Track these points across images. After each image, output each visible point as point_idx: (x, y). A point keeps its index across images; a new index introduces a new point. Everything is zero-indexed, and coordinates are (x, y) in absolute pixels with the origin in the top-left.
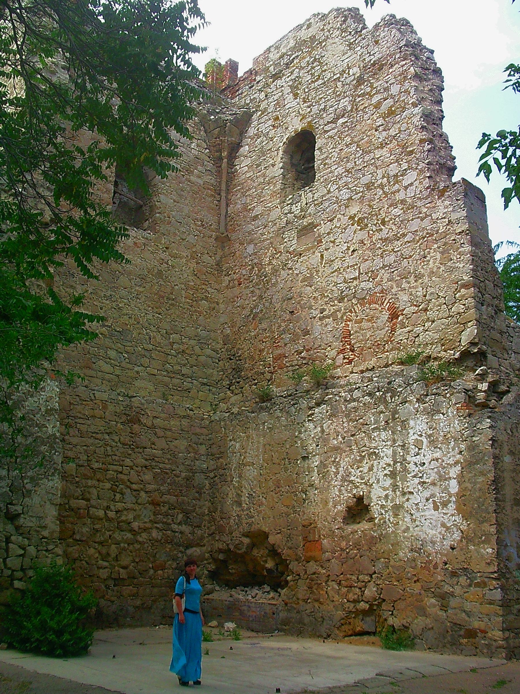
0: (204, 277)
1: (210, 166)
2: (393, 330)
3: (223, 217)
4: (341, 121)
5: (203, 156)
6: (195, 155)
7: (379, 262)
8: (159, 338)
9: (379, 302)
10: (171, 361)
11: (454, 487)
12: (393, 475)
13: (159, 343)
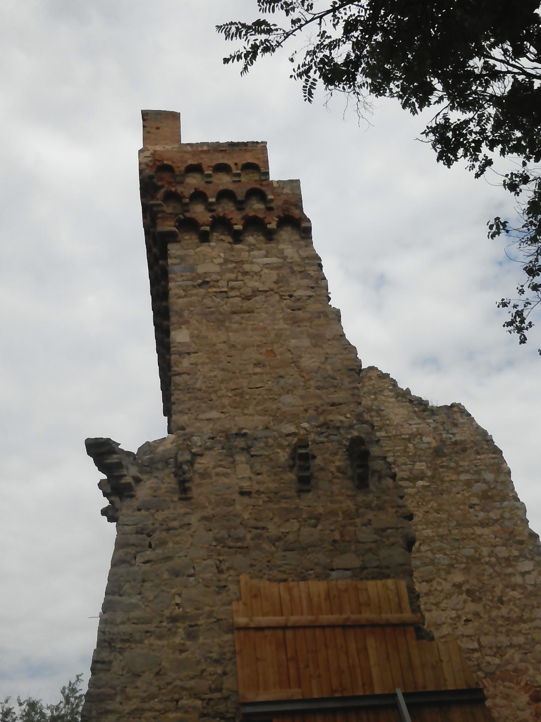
4: (420, 483)
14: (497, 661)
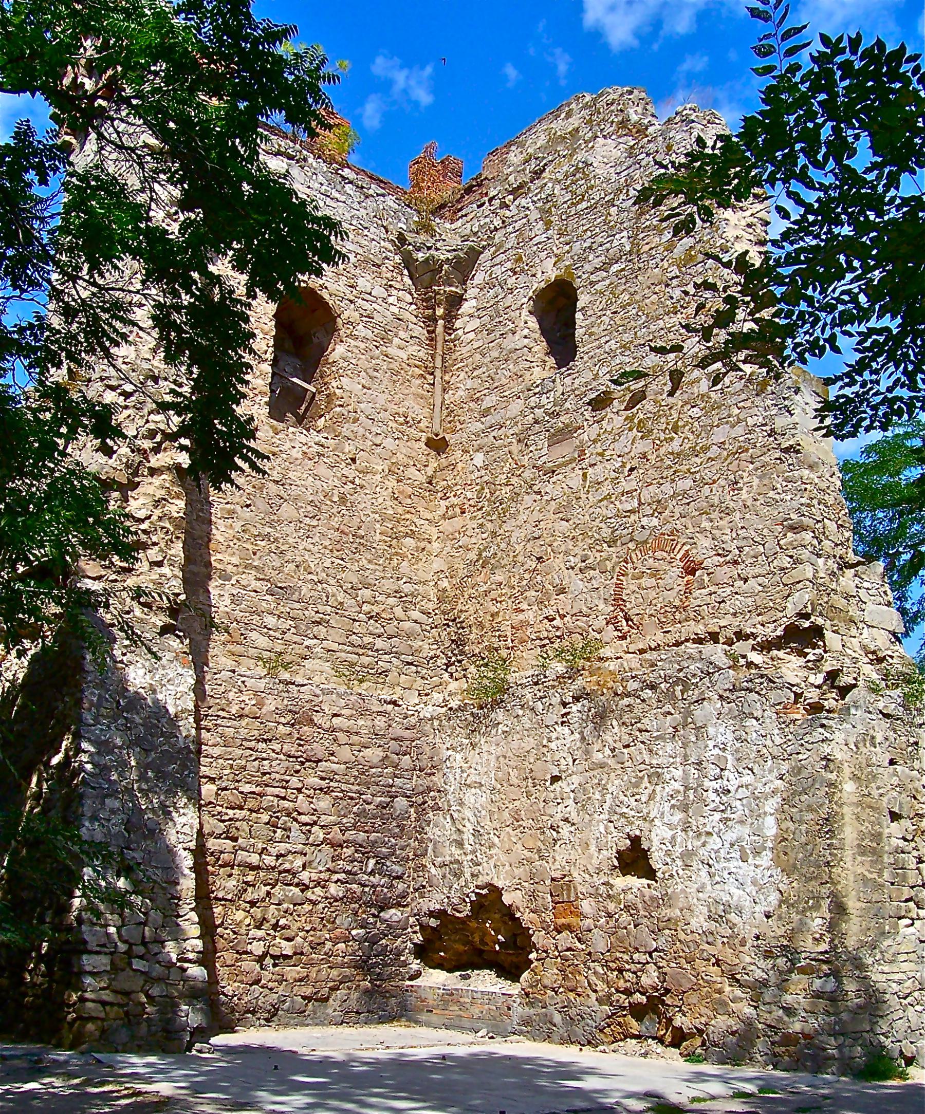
0: (409, 501)
1: (419, 331)
2: (688, 591)
3: (437, 409)
4: (615, 268)
5: (406, 315)
6: (393, 314)
7: (668, 489)
8: (341, 597)
9: (668, 549)
10: (360, 630)
11: (770, 827)
12: (685, 808)
13: (341, 604)
14: (655, 522)
